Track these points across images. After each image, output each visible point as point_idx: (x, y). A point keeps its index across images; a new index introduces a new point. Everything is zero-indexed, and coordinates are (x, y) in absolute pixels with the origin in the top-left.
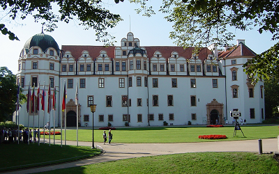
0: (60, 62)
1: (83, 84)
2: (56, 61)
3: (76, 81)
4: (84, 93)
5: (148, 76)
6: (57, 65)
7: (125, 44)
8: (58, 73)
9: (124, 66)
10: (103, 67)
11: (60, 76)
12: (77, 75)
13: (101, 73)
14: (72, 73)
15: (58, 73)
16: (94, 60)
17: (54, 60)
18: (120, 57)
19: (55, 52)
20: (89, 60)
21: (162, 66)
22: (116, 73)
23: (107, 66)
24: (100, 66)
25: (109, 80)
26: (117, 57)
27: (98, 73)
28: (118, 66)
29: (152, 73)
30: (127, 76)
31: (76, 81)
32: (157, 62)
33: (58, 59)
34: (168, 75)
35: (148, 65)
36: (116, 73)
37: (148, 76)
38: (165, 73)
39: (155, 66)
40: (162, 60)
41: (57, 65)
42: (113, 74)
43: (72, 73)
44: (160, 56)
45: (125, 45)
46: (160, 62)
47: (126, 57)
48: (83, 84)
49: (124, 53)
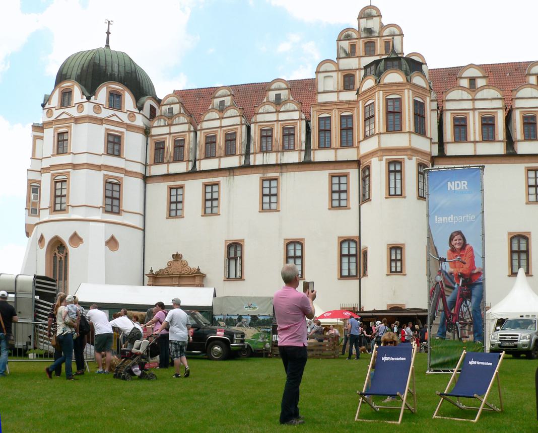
0: (147, 132)
1: (210, 204)
2: (129, 127)
3: (193, 190)
4: (220, 230)
5: (433, 160)
6: (134, 145)
7: (353, 47)
8: (139, 169)
9: (347, 129)
10: (277, 134)
11: (146, 179)
12: (194, 173)
13: (271, 159)
14: (181, 167)
15: (139, 169)
16: (247, 116)
17: (121, 124)
18: (332, 97)
19: (128, 100)
20: (232, 120)
21: (488, 124)
22: (320, 156)
23: (289, 133)
24: (266, 135)
25: (290, 182)
26: (322, 98)
27: (258, 159)
28: (325, 131)
29: (452, 149)
30: (358, 163)
31: (193, 190)
32: (468, 105)
33: (140, 121)
34: (511, 155)
35: (431, 120)
36: (320, 156)
37: (433, 160)
38: (499, 148)
39: (461, 125)
40: (490, 100)
41: (134, 145)
42: (307, 164)
43: (181, 167)
44: (480, 83)
45: (351, 54)
46: (479, 104)
47: (351, 96)
48: (210, 204)
49: (348, 81)
